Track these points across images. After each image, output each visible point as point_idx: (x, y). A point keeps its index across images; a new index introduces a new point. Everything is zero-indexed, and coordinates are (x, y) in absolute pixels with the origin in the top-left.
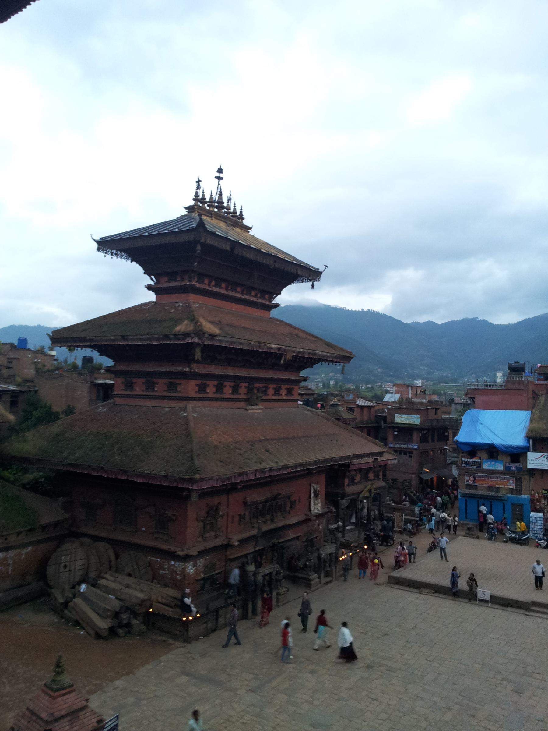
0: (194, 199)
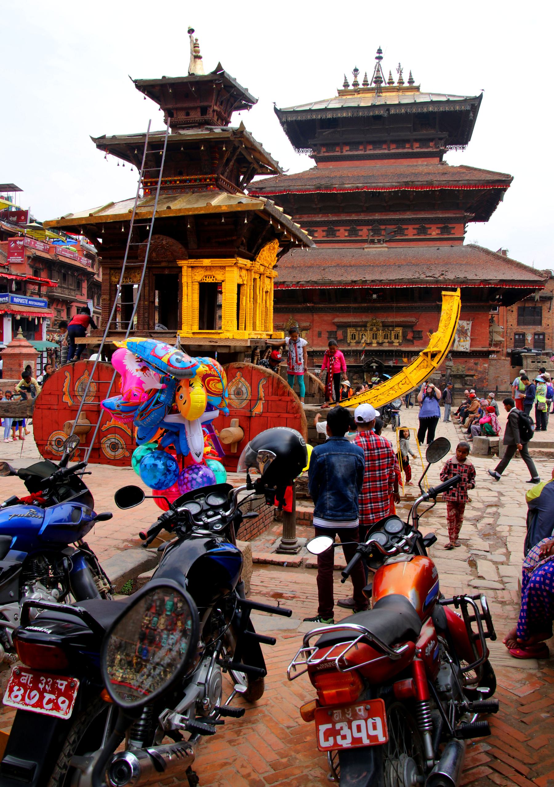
0: (344, 86)
